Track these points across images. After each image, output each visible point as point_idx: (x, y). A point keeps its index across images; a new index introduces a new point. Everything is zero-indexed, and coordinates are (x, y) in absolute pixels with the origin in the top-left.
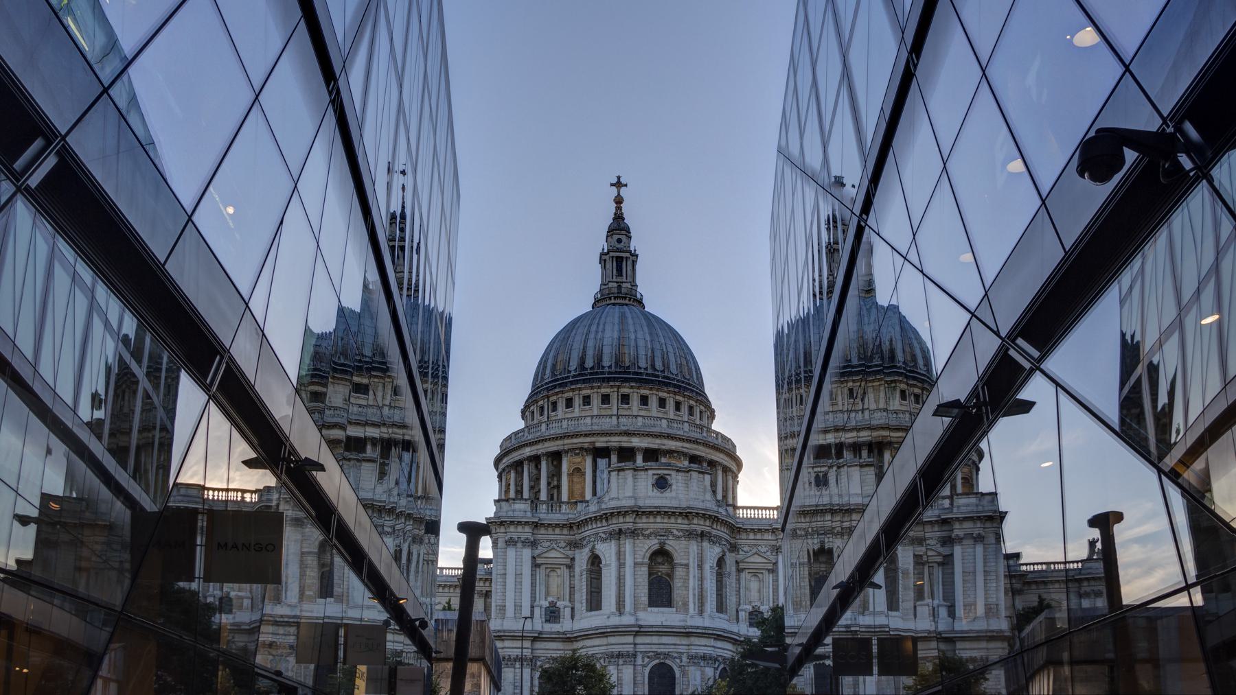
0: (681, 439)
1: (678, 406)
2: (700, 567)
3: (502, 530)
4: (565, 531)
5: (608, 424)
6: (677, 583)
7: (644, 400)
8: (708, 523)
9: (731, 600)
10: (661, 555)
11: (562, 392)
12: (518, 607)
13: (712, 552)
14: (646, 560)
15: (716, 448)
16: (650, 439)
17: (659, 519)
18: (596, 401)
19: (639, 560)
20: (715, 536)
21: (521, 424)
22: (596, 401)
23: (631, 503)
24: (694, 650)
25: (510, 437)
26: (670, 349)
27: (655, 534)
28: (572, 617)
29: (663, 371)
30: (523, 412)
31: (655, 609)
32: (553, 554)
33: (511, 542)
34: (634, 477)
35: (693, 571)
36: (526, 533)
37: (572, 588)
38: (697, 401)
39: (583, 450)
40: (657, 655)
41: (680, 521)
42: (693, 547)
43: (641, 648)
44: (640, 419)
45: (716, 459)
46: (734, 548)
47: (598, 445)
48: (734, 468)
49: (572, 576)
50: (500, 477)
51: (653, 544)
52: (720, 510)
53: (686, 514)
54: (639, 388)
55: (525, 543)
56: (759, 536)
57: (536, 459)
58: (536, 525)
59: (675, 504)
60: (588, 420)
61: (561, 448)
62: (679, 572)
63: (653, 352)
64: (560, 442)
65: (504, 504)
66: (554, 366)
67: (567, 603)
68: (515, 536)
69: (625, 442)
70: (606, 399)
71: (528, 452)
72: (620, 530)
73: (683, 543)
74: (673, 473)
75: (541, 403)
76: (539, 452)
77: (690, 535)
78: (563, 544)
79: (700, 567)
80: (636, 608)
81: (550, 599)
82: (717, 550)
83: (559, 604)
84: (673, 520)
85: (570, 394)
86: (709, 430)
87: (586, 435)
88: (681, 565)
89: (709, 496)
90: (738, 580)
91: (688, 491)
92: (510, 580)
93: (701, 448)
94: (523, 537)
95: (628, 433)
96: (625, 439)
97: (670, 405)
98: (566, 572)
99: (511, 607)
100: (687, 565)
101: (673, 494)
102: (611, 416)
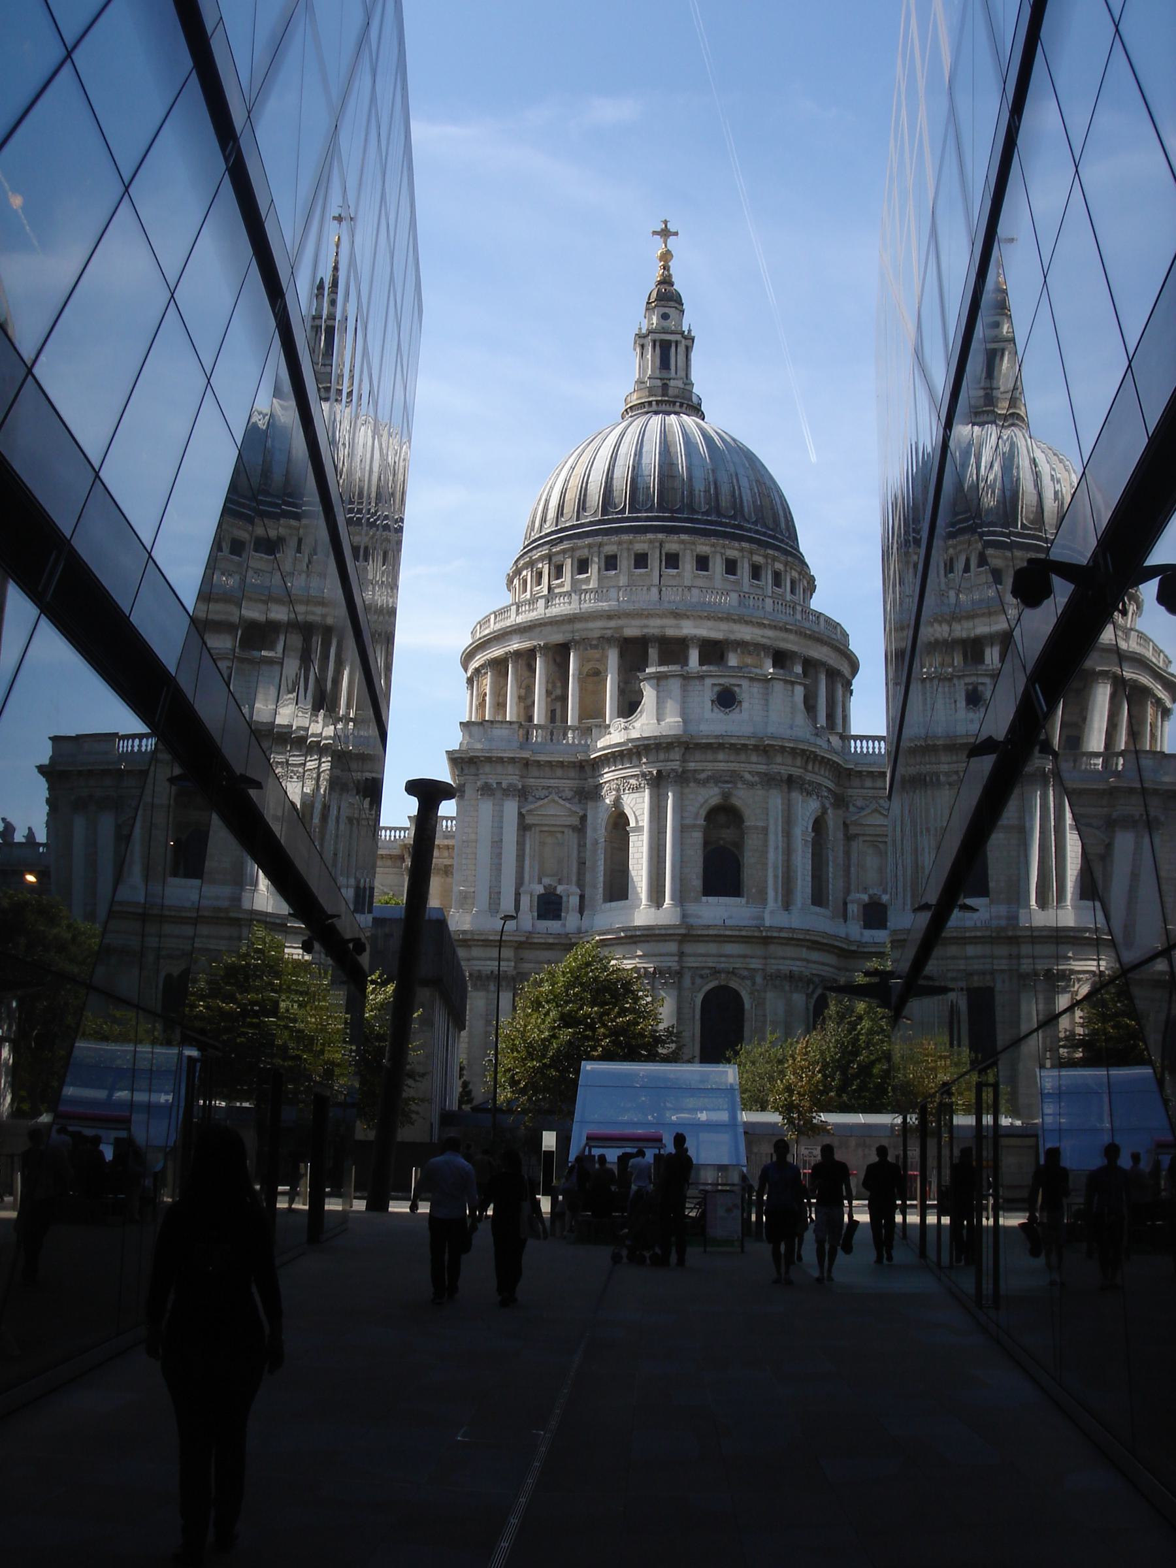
0: (761, 625)
1: (756, 572)
2: (788, 835)
3: (473, 770)
4: (572, 773)
5: (647, 598)
6: (749, 859)
8: (799, 762)
9: (835, 885)
10: (724, 816)
13: (807, 809)
14: (701, 822)
16: (710, 624)
17: (721, 756)
18: (625, 563)
19: (688, 821)
20: (811, 783)
22: (625, 563)
24: (774, 966)
25: (484, 622)
26: (744, 482)
27: (715, 779)
28: (581, 911)
29: (734, 517)
30: (510, 581)
34: (684, 690)
35: (775, 839)
36: (511, 777)
37: (582, 863)
38: (786, 565)
40: (715, 972)
41: (754, 758)
42: (776, 800)
43: (691, 962)
44: (695, 591)
46: (840, 801)
48: (846, 670)
49: (582, 846)
50: (470, 681)
51: (711, 796)
52: (819, 741)
53: (765, 750)
54: (694, 543)
55: (508, 792)
57: (526, 658)
58: (527, 764)
59: (747, 730)
61: (569, 636)
62: (751, 842)
63: (716, 488)
64: (568, 627)
65: (475, 729)
68: (493, 781)
70: (641, 560)
71: (515, 645)
72: (659, 772)
73: (760, 792)
74: (745, 683)
77: (769, 781)
78: (569, 794)
79: (788, 835)
80: (681, 898)
81: (547, 881)
83: (560, 889)
84: (743, 757)
86: (807, 611)
88: (756, 828)
89: (801, 717)
90: (847, 854)
91: (771, 711)
93: (792, 637)
95: (677, 615)
96: (670, 622)
97: (744, 570)
98: (572, 838)
100: (765, 830)
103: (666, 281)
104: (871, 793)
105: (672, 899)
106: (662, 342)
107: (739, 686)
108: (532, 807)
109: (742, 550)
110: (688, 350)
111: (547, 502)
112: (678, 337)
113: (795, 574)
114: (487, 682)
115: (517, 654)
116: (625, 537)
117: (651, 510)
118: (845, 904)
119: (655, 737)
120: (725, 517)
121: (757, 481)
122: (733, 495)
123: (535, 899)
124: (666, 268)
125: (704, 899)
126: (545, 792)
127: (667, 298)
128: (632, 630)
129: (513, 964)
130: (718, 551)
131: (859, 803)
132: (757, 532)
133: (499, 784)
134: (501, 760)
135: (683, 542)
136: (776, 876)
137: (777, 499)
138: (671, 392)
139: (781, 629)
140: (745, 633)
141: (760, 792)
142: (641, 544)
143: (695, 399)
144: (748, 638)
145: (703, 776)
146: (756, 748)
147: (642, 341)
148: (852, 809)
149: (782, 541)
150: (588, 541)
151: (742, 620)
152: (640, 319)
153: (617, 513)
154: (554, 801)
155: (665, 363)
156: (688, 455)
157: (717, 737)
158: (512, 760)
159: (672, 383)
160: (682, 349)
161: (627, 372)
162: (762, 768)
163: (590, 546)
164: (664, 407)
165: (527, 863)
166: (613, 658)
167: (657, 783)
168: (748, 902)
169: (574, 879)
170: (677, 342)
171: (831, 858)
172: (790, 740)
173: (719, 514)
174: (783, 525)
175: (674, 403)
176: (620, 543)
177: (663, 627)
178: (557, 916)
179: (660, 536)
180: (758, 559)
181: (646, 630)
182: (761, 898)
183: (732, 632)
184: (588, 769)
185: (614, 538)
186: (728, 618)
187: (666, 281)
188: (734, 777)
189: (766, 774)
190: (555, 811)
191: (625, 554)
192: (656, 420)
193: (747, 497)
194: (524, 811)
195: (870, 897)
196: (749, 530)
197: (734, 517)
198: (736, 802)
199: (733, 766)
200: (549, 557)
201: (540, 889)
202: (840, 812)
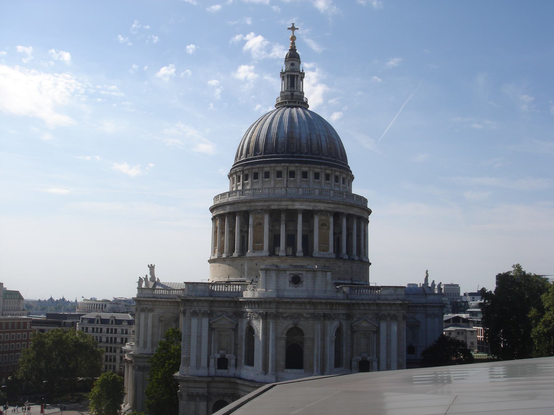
1: (327, 177)
2: (323, 339)
6: (306, 352)
7: (305, 175)
8: (328, 307)
11: (252, 169)
12: (198, 360)
13: (332, 326)
14: (284, 336)
15: (353, 206)
16: (307, 203)
17: (293, 306)
18: (273, 176)
21: (188, 255)
23: (274, 295)
26: (323, 138)
27: (291, 316)
28: (236, 366)
31: (289, 371)
33: (195, 314)
37: (236, 344)
38: (340, 172)
39: (263, 211)
41: (308, 307)
42: (318, 326)
44: (301, 190)
45: (351, 212)
47: (273, 207)
49: (236, 336)
50: (212, 219)
51: (288, 324)
53: (312, 302)
54: (301, 167)
55: (205, 314)
57: (232, 215)
59: (305, 295)
61: (248, 208)
64: (248, 204)
68: (197, 309)
70: (279, 174)
71: (228, 209)
72: (266, 313)
74: (304, 273)
75: (238, 174)
77: (315, 317)
79: (323, 339)
81: (221, 352)
82: (336, 324)
83: (227, 356)
87: (265, 201)
92: (194, 340)
93: (341, 206)
95: (293, 200)
96: (290, 203)
97: (323, 176)
101: (304, 288)
102: (281, 188)
103: (293, 50)
106: (291, 75)
107: (302, 274)
108: (214, 320)
109: (321, 169)
110: (302, 80)
112: (298, 74)
115: (229, 214)
116: (272, 165)
117: (282, 153)
118: (351, 362)
119: (264, 299)
122: (318, 144)
124: (293, 43)
125: (286, 370)
127: (293, 57)
129: (206, 390)
130: (311, 170)
132: (328, 160)
133: (200, 311)
135: (296, 166)
136: (317, 360)
139: (337, 204)
140: (321, 206)
142: (279, 167)
143: (305, 100)
144: (323, 208)
146: (309, 303)
147: (283, 75)
148: (355, 319)
149: (339, 163)
150: (258, 166)
151: (320, 201)
152: (282, 66)
159: (295, 93)
160: (299, 78)
161: (277, 86)
162: (312, 311)
163: (258, 168)
164: (291, 104)
165: (213, 344)
166: (266, 219)
167: (265, 317)
168: (305, 372)
169: (233, 352)
170: (297, 76)
172: (324, 299)
174: (340, 154)
175: (296, 102)
176: (271, 167)
177: (287, 205)
178: (226, 368)
179: (287, 164)
180: (328, 172)
181: (280, 207)
183: (316, 206)
185: (268, 165)
186: (315, 201)
187: (293, 50)
189: (314, 314)
190: (225, 322)
191: (273, 172)
192: (288, 110)
193: (324, 144)
194: (211, 322)
196: (325, 160)
198: (300, 327)
200: (243, 171)
201: (218, 356)
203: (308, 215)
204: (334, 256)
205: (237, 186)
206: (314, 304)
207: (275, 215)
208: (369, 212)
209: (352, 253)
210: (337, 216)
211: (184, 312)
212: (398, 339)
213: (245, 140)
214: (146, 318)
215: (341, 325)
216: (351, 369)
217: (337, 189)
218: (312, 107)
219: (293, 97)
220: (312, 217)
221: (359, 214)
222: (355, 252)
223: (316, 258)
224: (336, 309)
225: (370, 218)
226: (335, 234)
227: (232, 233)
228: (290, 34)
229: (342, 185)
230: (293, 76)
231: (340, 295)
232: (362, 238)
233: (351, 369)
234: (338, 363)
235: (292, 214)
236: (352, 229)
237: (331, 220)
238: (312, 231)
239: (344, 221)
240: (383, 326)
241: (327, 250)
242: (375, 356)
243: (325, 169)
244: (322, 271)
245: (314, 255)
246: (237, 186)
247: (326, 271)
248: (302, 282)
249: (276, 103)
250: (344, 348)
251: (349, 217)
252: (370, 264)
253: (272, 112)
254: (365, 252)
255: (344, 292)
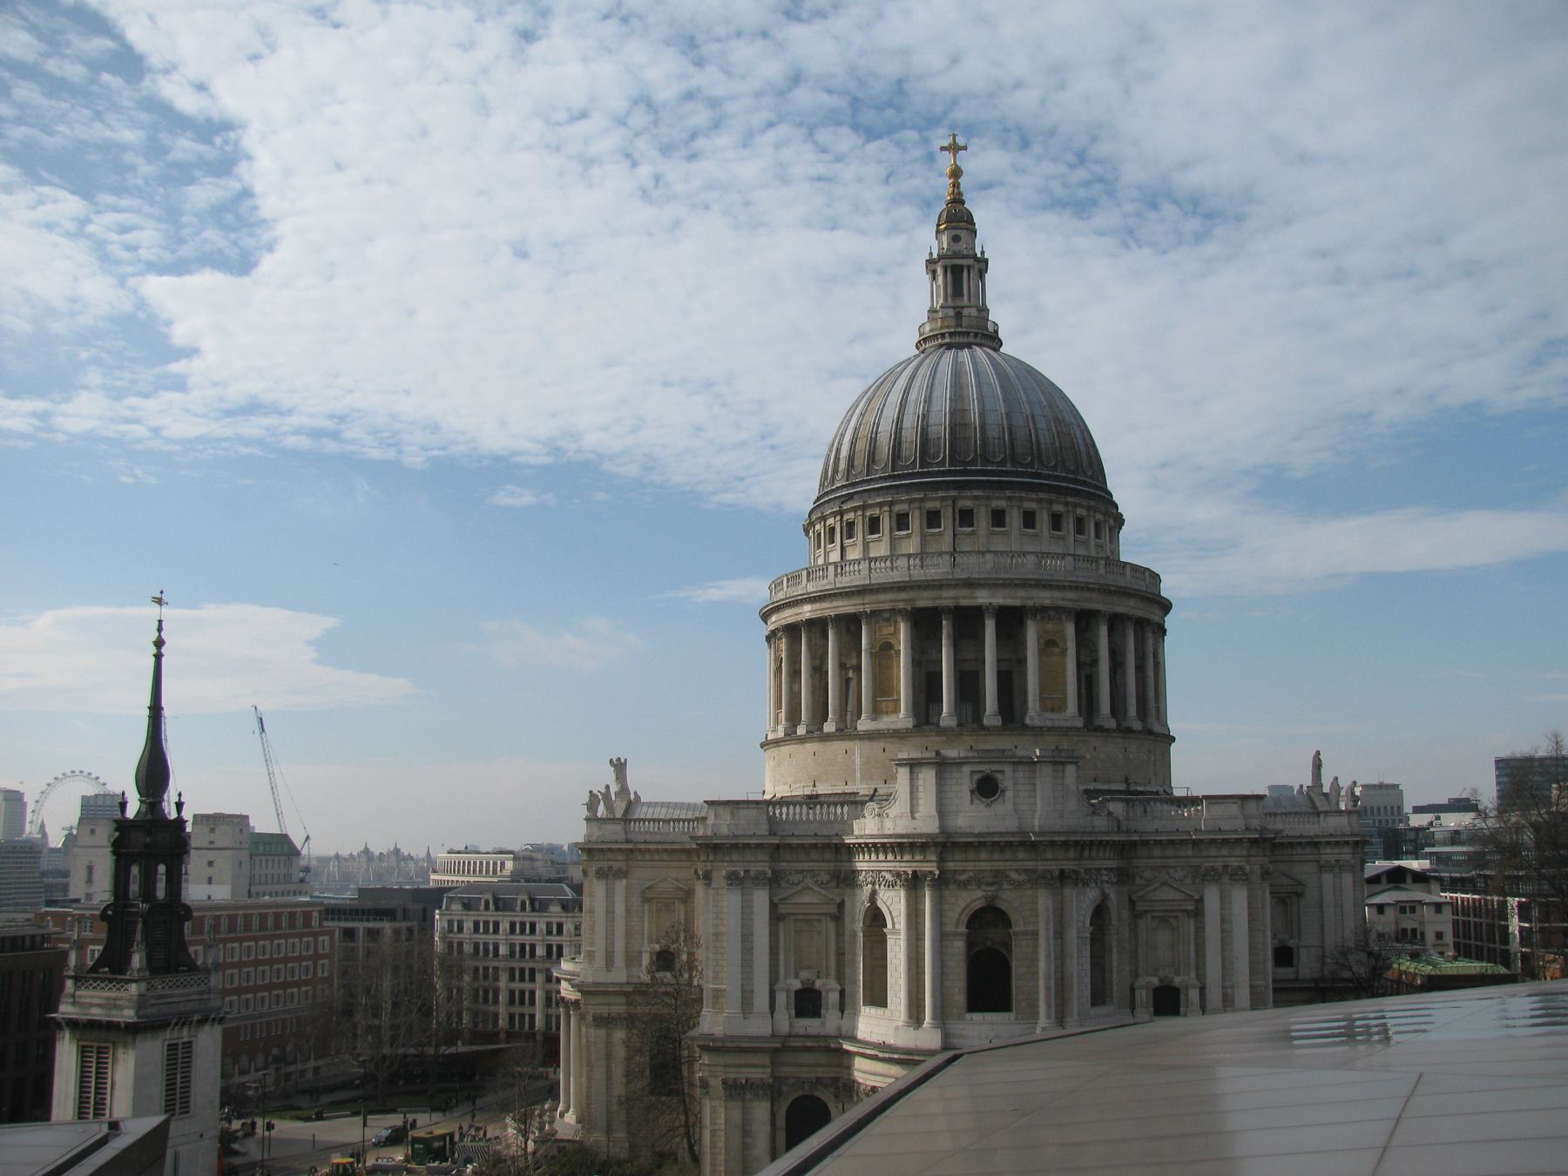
2: (1060, 934)
4: (828, 856)
6: (1017, 968)
7: (998, 518)
8: (1072, 854)
10: (988, 919)
11: (864, 508)
13: (1081, 903)
14: (963, 929)
16: (1006, 591)
17: (984, 855)
19: (950, 928)
22: (915, 521)
26: (1042, 424)
28: (842, 1010)
29: (1031, 465)
31: (977, 1016)
32: (806, 899)
35: (1044, 945)
36: (761, 865)
37: (840, 954)
38: (1089, 508)
41: (1021, 855)
42: (1044, 900)
45: (1121, 610)
47: (921, 604)
49: (840, 934)
50: (768, 639)
54: (988, 498)
55: (758, 880)
56: (1169, 852)
57: (817, 626)
59: (1011, 824)
60: (902, 562)
61: (860, 609)
63: (1010, 433)
66: (851, 459)
67: (834, 984)
69: (968, 599)
71: (807, 612)
72: (915, 872)
74: (1008, 770)
76: (827, 613)
77: (1039, 879)
78: (825, 877)
79: (1060, 934)
80: (942, 1016)
81: (804, 974)
82: (1091, 895)
83: (818, 984)
84: (1008, 855)
85: (877, 511)
86: (1113, 562)
88: (1025, 933)
90: (1134, 931)
93: (1095, 596)
94: (755, 868)
96: (964, 592)
97: (1043, 521)
98: (832, 927)
99: (732, 1003)
103: (957, 200)
104: (1159, 862)
105: (934, 1017)
110: (982, 273)
111: (838, 450)
112: (970, 262)
113: (1099, 516)
114: (783, 644)
115: (811, 623)
118: (1132, 990)
120: (1022, 465)
121: (1056, 420)
123: (792, 995)
124: (956, 185)
125: (968, 1016)
126: (800, 877)
128: (924, 600)
131: (1147, 874)
132: (1056, 478)
134: (747, 846)
135: (976, 498)
136: (1048, 989)
137: (1078, 433)
138: (965, 322)
140: (1045, 597)
141: (1029, 892)
144: (1047, 602)
145: (963, 877)
147: (932, 267)
148: (1138, 881)
149: (1084, 483)
153: (907, 467)
154: (807, 888)
155: (957, 291)
156: (981, 399)
157: (979, 835)
158: (760, 846)
159: (965, 312)
161: (919, 296)
162: (1029, 865)
165: (782, 957)
167: (913, 883)
169: (833, 972)
170: (969, 267)
171: (1114, 944)
172: (1059, 833)
173: (1014, 462)
174: (1085, 463)
178: (816, 1012)
179: (952, 493)
182: (1033, 1014)
184: (843, 851)
186: (1025, 584)
188: (999, 877)
191: (917, 513)
192: (949, 356)
194: (776, 900)
195: (1161, 980)
197: (1031, 465)
198: (1003, 906)
199: (1001, 866)
201: (797, 985)
202: (1125, 889)
203: (1011, 621)
204: (1079, 723)
205: (826, 554)
206: (1033, 846)
207: (925, 623)
208: (1166, 606)
209: (1126, 712)
210: (1084, 620)
211: (707, 877)
212: (1250, 929)
213: (843, 436)
214: (610, 894)
215: (1105, 897)
216: (1133, 1009)
217: (1081, 551)
218: (1011, 347)
219: (963, 321)
220: (1021, 623)
221: (1140, 613)
222: (1132, 710)
223: (1033, 728)
224: (1090, 858)
225: (1170, 621)
226: (1079, 665)
227: (819, 671)
228: (946, 161)
229: (1092, 542)
230: (960, 270)
231: (1101, 822)
232: (1151, 673)
233: (1133, 1009)
234: (1099, 996)
235: (968, 621)
236: (1124, 654)
237: (1070, 630)
238: (1022, 661)
239: (1103, 632)
240: (1212, 897)
241: (1061, 707)
242: (1193, 975)
243: (1051, 502)
244: (1055, 763)
245: (1028, 721)
246: (826, 554)
247: (1063, 763)
248: (1003, 791)
249: (917, 338)
250: (1115, 957)
251: (1115, 621)
252: (1174, 739)
253: (910, 361)
254: (1158, 709)
255: (1110, 814)
